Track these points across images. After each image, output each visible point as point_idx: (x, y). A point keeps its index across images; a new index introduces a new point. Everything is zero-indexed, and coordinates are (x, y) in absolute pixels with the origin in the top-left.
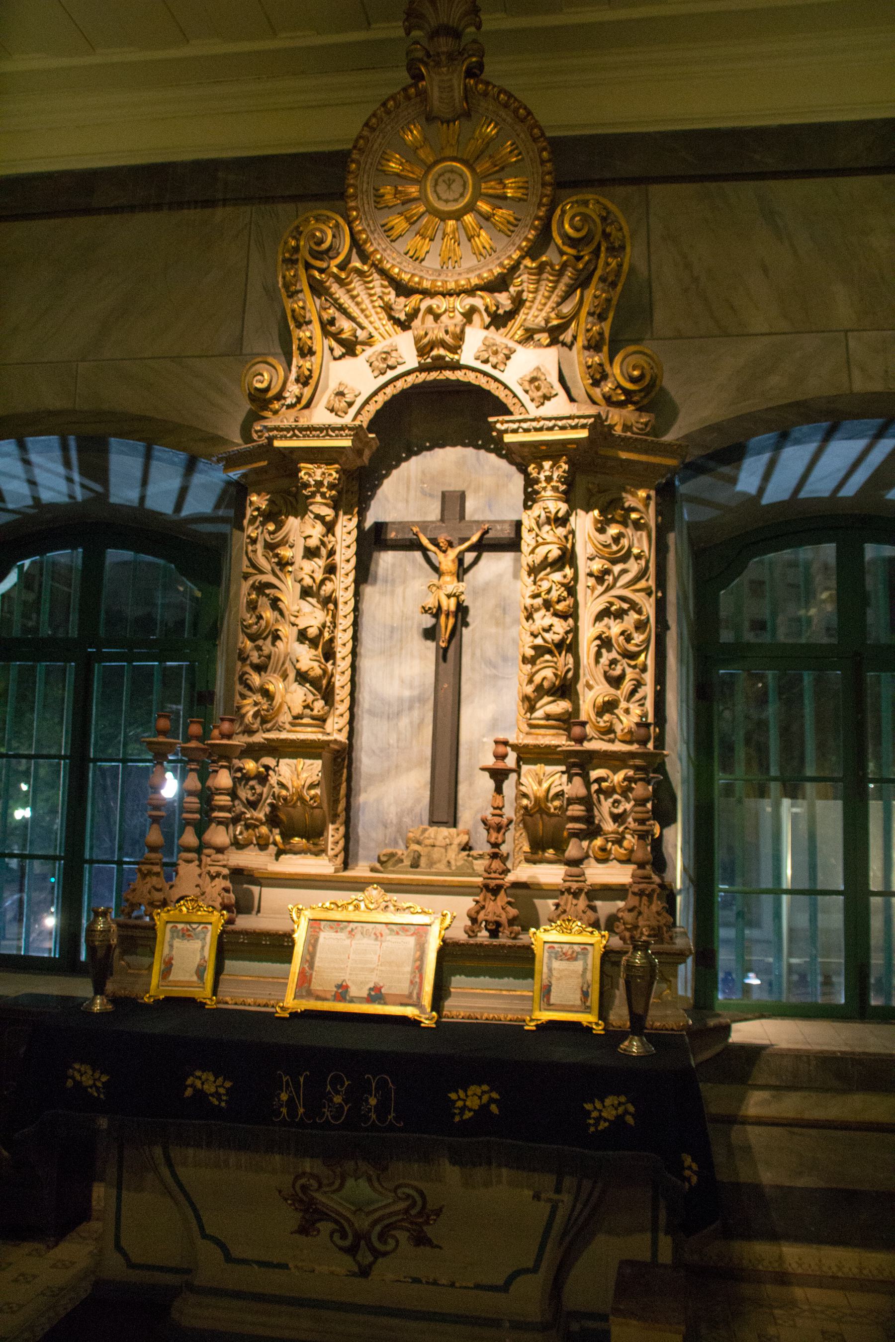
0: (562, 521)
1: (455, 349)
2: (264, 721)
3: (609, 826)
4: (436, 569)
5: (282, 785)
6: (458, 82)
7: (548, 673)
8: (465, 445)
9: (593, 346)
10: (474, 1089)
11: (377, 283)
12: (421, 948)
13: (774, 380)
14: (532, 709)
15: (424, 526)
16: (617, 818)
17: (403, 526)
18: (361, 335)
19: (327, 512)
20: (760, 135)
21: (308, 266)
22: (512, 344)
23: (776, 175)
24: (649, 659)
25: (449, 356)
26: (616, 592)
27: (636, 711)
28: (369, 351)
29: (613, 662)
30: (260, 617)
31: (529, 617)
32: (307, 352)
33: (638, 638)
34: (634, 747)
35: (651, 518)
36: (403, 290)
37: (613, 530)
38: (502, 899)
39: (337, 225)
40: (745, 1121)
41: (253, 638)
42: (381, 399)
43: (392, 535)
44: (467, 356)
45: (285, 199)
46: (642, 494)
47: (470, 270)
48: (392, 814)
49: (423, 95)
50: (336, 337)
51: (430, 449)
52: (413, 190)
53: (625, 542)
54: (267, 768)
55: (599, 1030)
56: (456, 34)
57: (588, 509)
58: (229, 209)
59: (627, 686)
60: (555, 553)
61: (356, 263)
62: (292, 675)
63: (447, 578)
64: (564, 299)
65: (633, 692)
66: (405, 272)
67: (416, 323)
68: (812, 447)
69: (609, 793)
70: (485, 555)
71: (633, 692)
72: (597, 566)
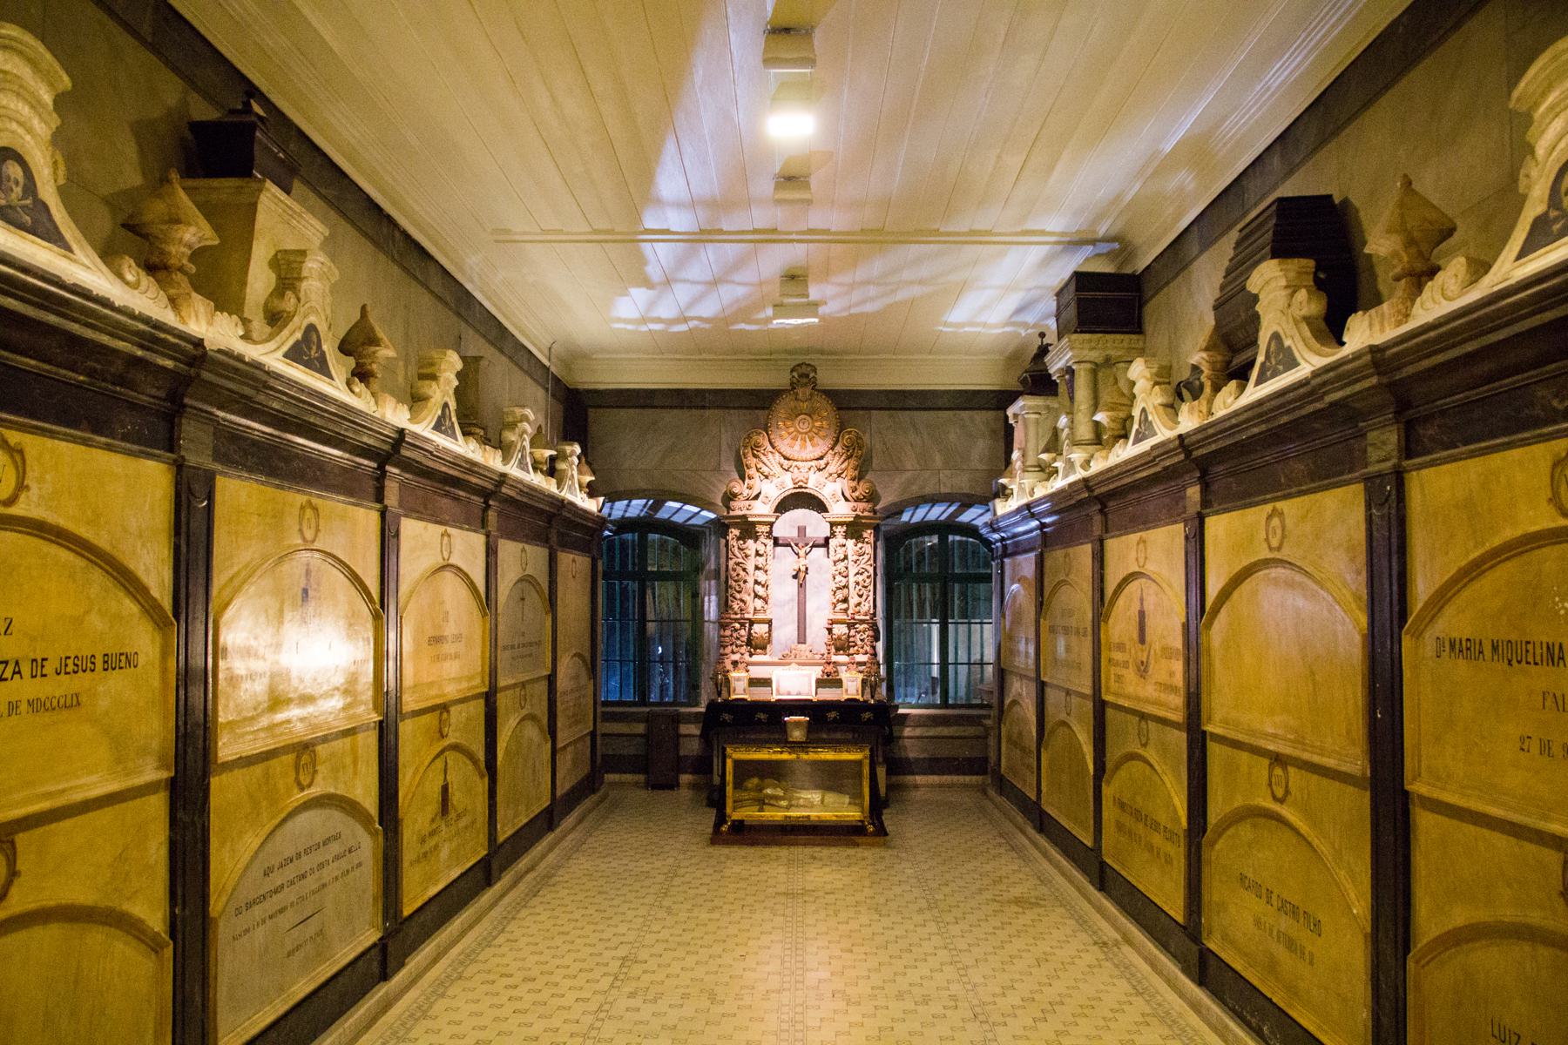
0: (844, 546)
2: (741, 610)
3: (859, 643)
4: (797, 554)
6: (808, 391)
9: (853, 479)
11: (777, 454)
12: (810, 680)
13: (914, 488)
16: (861, 640)
17: (785, 539)
19: (765, 541)
20: (911, 393)
21: (752, 449)
23: (917, 409)
24: (871, 588)
27: (867, 605)
28: (776, 481)
30: (738, 575)
32: (750, 478)
33: (868, 581)
34: (868, 618)
35: (872, 540)
36: (786, 458)
37: (860, 545)
38: (831, 665)
40: (904, 738)
41: (736, 581)
42: (780, 498)
43: (781, 542)
45: (734, 408)
46: (869, 531)
47: (811, 452)
49: (797, 394)
52: (789, 423)
55: (861, 699)
58: (712, 411)
59: (864, 597)
60: (842, 557)
61: (769, 448)
62: (753, 595)
66: (787, 451)
68: (927, 509)
70: (814, 549)
72: (855, 557)
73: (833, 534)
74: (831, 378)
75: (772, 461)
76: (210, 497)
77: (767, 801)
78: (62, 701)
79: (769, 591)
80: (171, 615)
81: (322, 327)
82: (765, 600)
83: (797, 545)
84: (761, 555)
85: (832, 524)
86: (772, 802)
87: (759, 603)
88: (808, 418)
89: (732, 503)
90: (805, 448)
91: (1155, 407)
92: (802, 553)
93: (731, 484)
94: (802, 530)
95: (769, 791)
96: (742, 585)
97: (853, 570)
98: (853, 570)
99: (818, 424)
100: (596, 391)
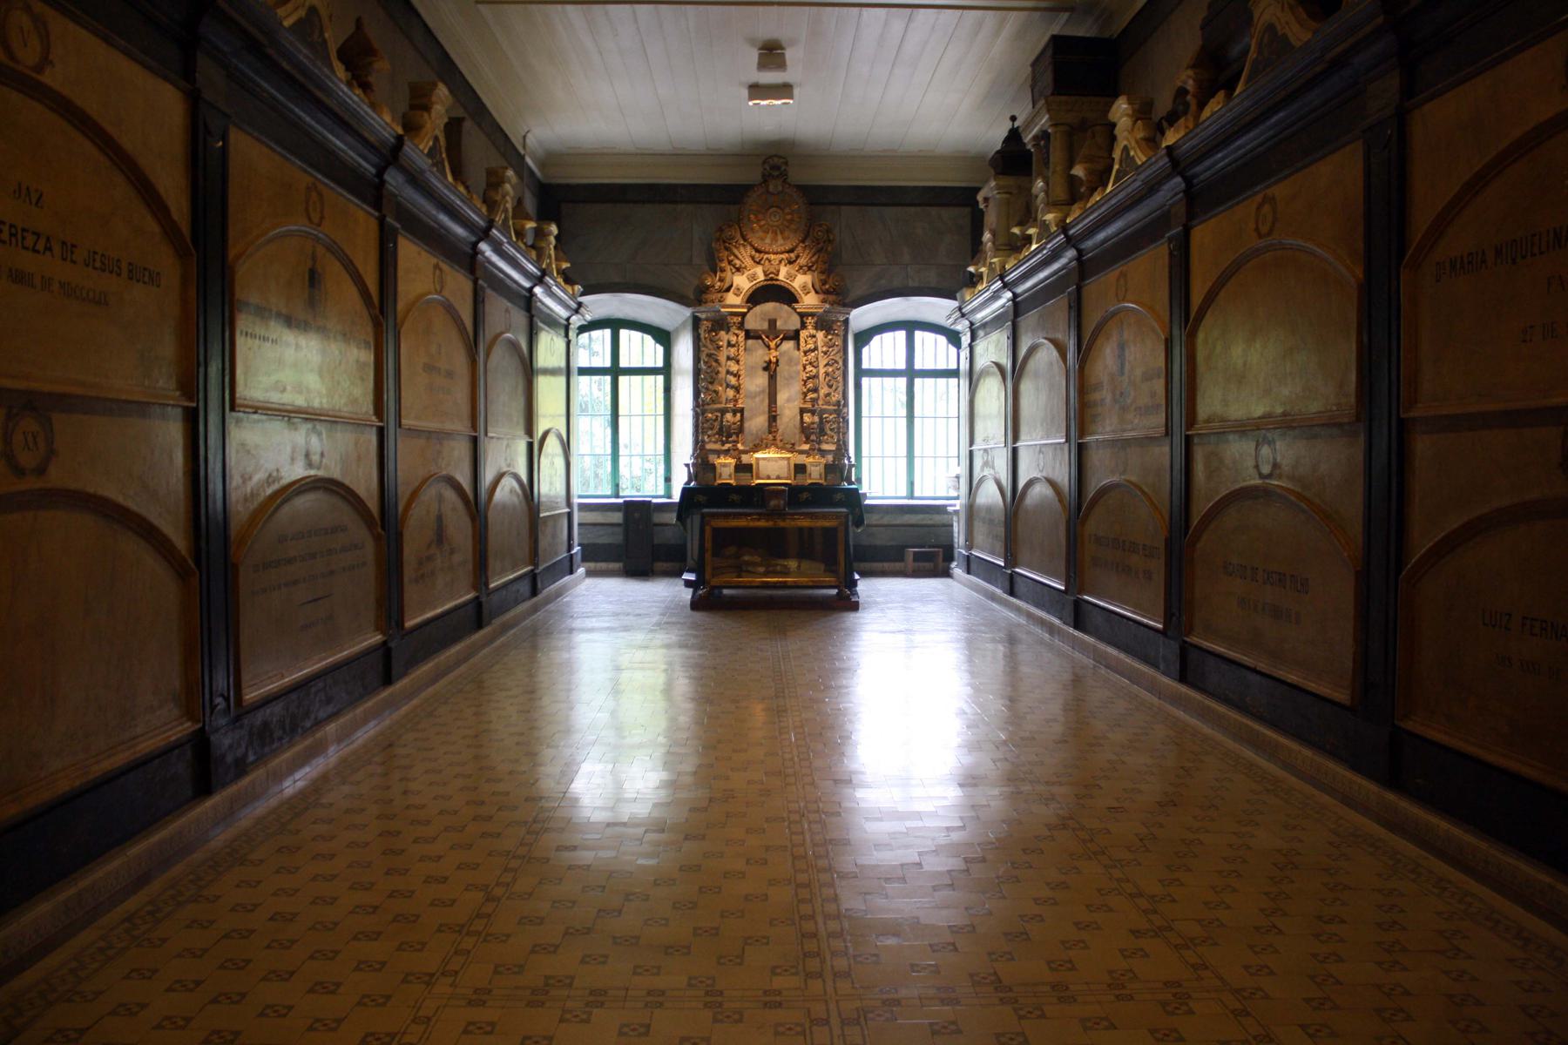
0: (814, 336)
1: (778, 275)
4: (769, 347)
5: (728, 421)
7: (811, 385)
8: (776, 302)
9: (822, 273)
10: (805, 493)
11: (749, 247)
13: (883, 282)
14: (806, 396)
15: (763, 331)
17: (756, 331)
18: (743, 266)
19: (737, 332)
21: (724, 242)
22: (796, 273)
24: (840, 379)
25: (776, 277)
26: (831, 357)
28: (747, 273)
29: (830, 380)
31: (805, 368)
37: (830, 337)
39: (735, 229)
43: (752, 334)
44: (781, 277)
45: (706, 203)
47: (781, 245)
48: (754, 432)
50: (734, 266)
51: (764, 302)
52: (760, 216)
53: (833, 341)
54: (717, 416)
56: (778, 168)
57: (822, 330)
62: (725, 385)
63: (772, 351)
64: (813, 256)
65: (836, 390)
67: (762, 262)
69: (828, 422)
71: (836, 390)
72: (824, 349)
73: (804, 326)
74: (798, 176)
75: (744, 255)
76: (224, 138)
77: (744, 568)
78: (91, 294)
79: (741, 382)
80: (188, 240)
81: (324, 13)
82: (737, 389)
83: (767, 337)
84: (733, 346)
85: (802, 316)
86: (750, 569)
87: (731, 393)
88: (779, 211)
89: (704, 296)
90: (776, 241)
91: (1137, 142)
92: (772, 344)
93: (703, 277)
94: (773, 323)
95: (746, 558)
96: (715, 376)
97: (822, 362)
98: (822, 362)
99: (789, 217)
100: (569, 187)
